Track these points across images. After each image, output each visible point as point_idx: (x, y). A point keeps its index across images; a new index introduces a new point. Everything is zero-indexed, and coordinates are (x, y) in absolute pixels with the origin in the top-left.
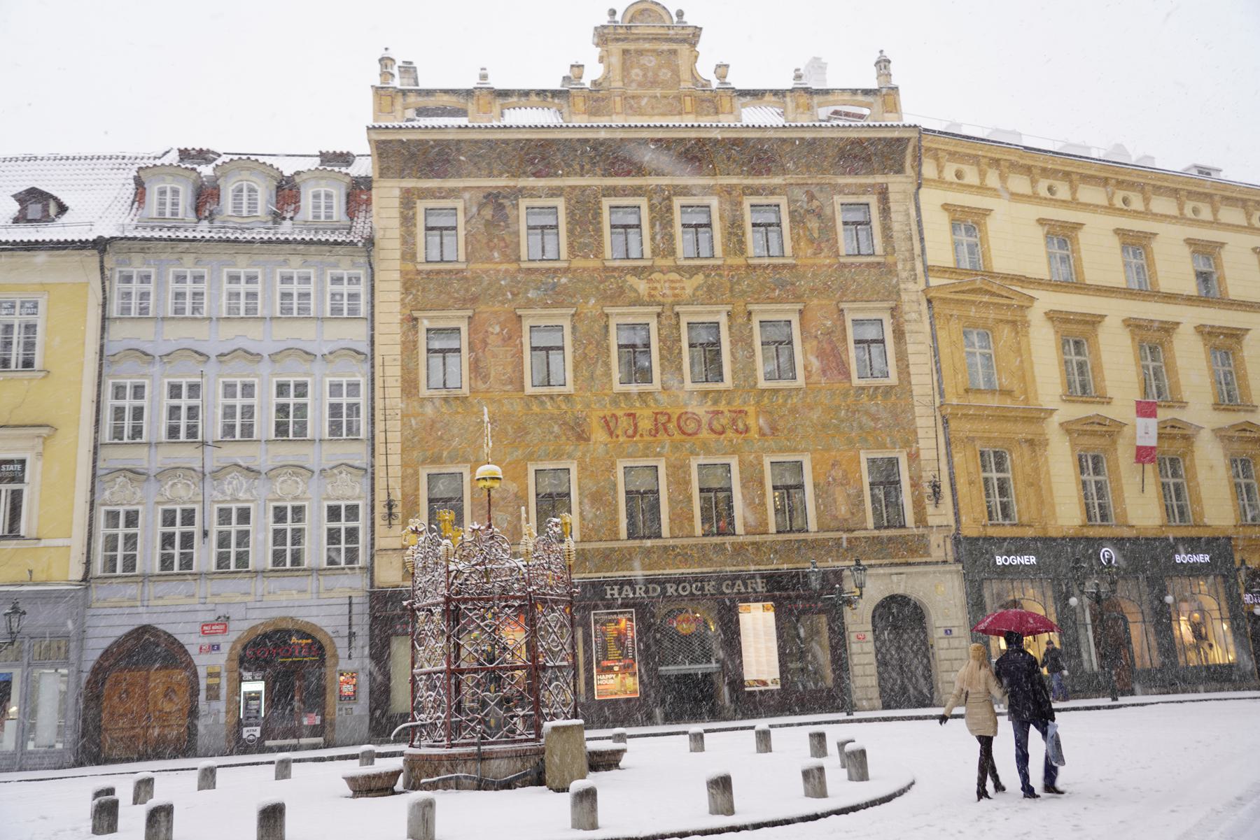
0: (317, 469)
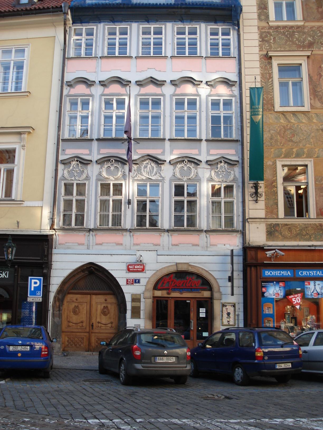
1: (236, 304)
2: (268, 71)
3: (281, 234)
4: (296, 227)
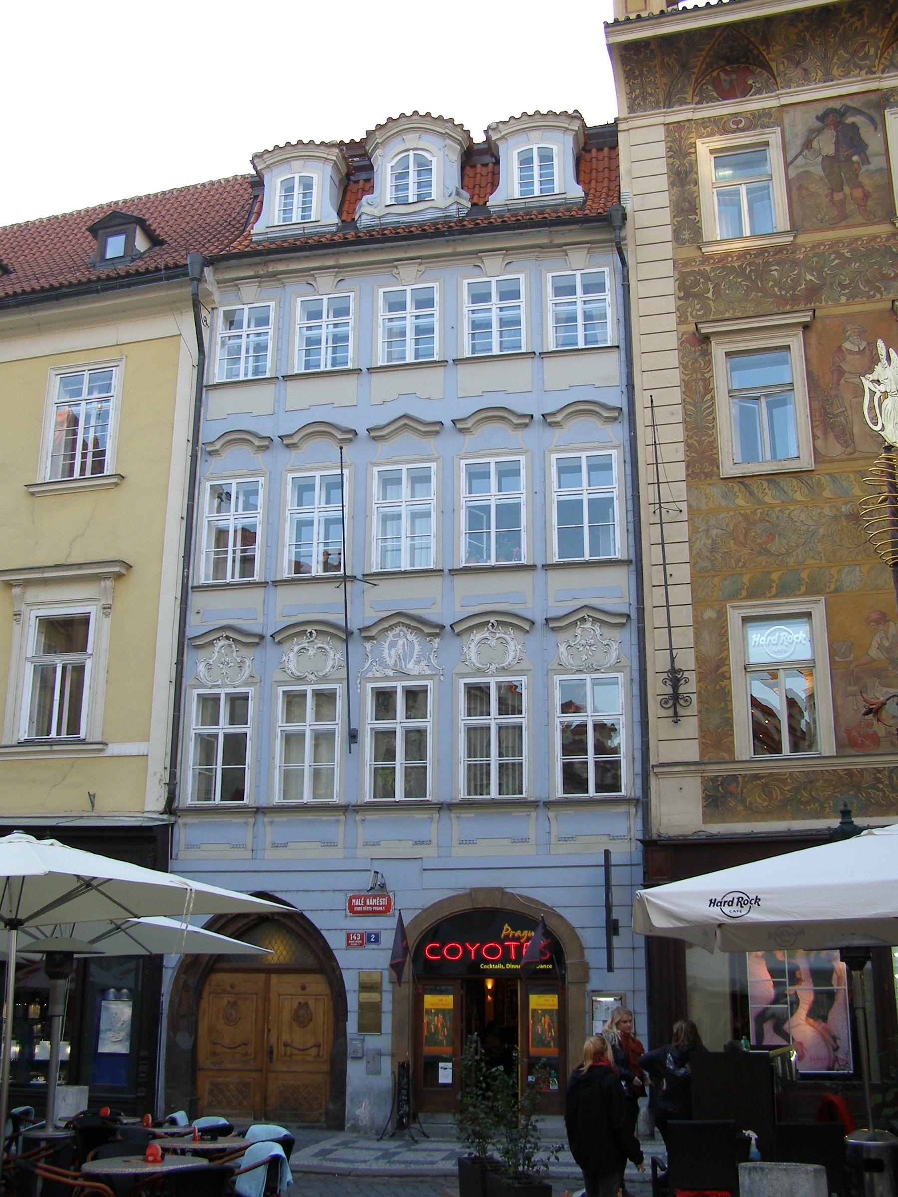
0: (539, 619)
1: (629, 995)
2: (703, 374)
3: (743, 801)
4: (784, 781)
